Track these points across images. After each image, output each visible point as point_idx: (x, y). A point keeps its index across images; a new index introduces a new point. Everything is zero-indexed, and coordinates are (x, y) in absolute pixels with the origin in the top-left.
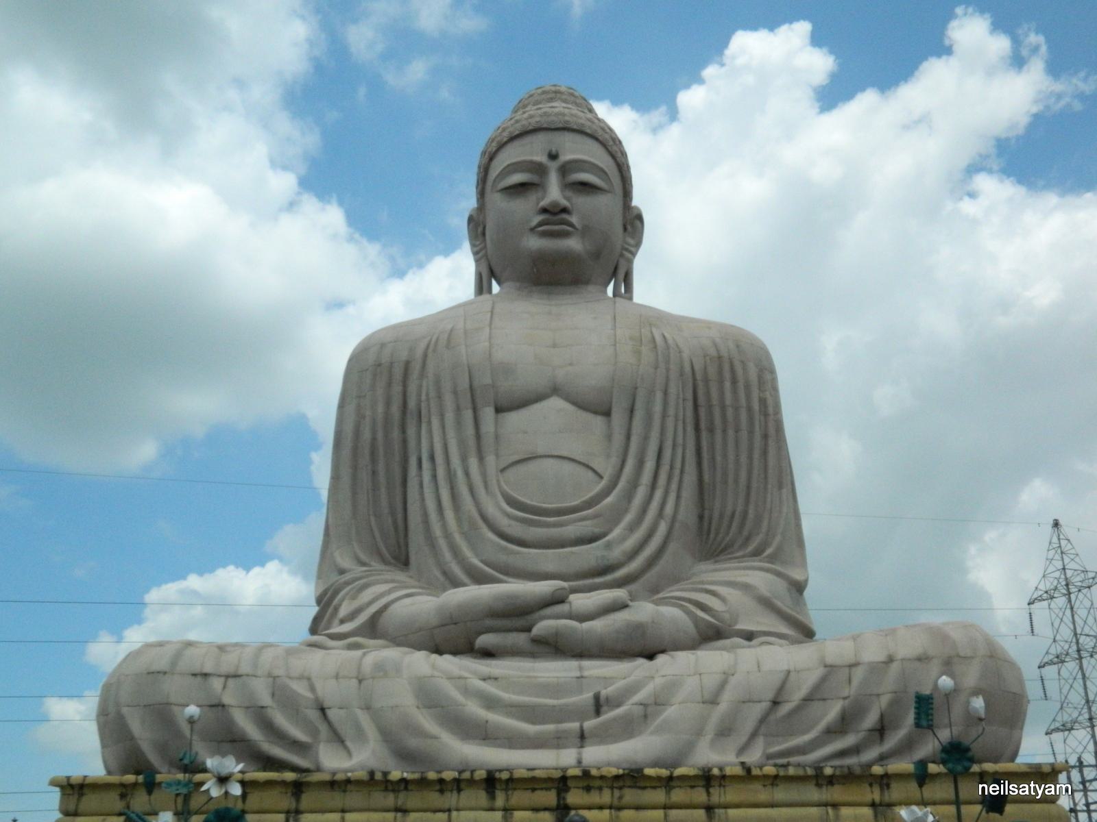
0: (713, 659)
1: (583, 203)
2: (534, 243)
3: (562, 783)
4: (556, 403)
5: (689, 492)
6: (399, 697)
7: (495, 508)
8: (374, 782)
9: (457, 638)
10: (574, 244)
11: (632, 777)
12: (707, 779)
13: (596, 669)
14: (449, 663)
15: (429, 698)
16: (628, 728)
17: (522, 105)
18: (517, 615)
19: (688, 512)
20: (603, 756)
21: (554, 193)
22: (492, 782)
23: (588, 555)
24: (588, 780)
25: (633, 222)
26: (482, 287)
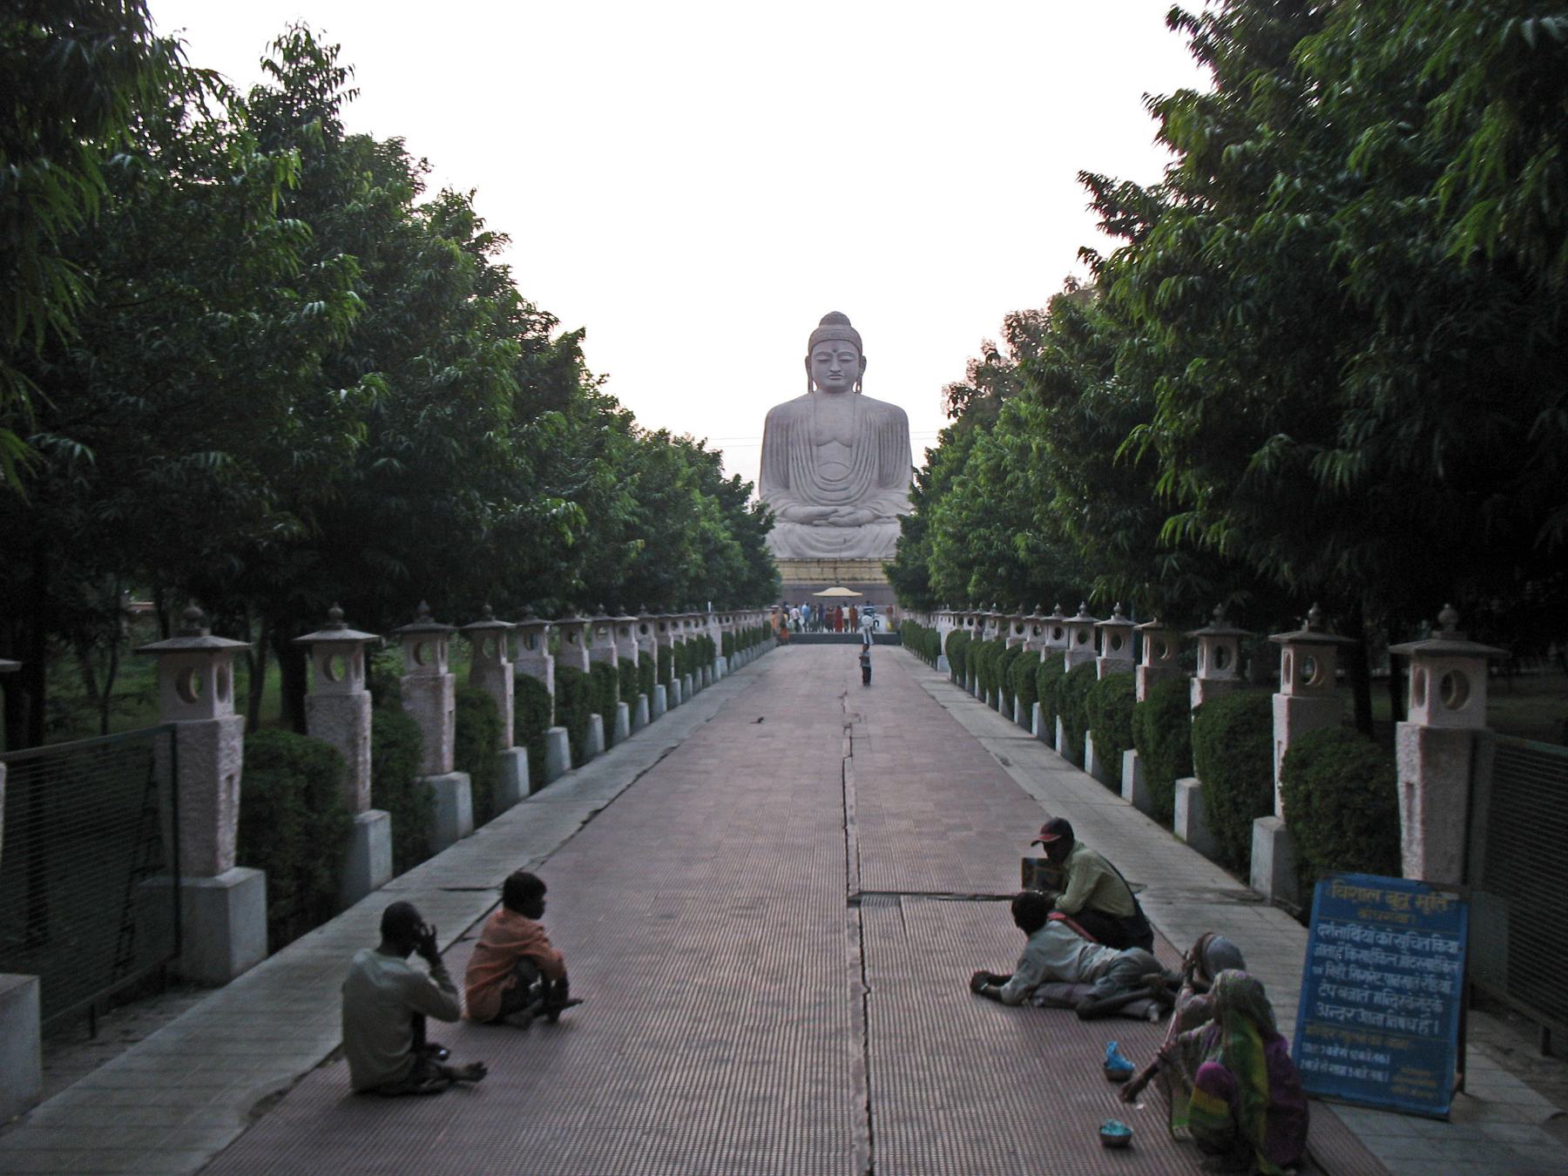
0: (875, 529)
1: (845, 366)
2: (829, 382)
3: (835, 561)
4: (836, 444)
5: (876, 471)
6: (794, 539)
7: (817, 479)
8: (791, 561)
9: (808, 521)
10: (842, 382)
11: (853, 560)
12: (870, 561)
13: (847, 531)
14: (806, 529)
15: (802, 539)
16: (851, 548)
17: (823, 321)
18: (824, 516)
19: (875, 476)
20: (845, 554)
21: (835, 367)
22: (819, 561)
23: (843, 494)
24: (842, 561)
25: (863, 362)
26: (810, 387)
